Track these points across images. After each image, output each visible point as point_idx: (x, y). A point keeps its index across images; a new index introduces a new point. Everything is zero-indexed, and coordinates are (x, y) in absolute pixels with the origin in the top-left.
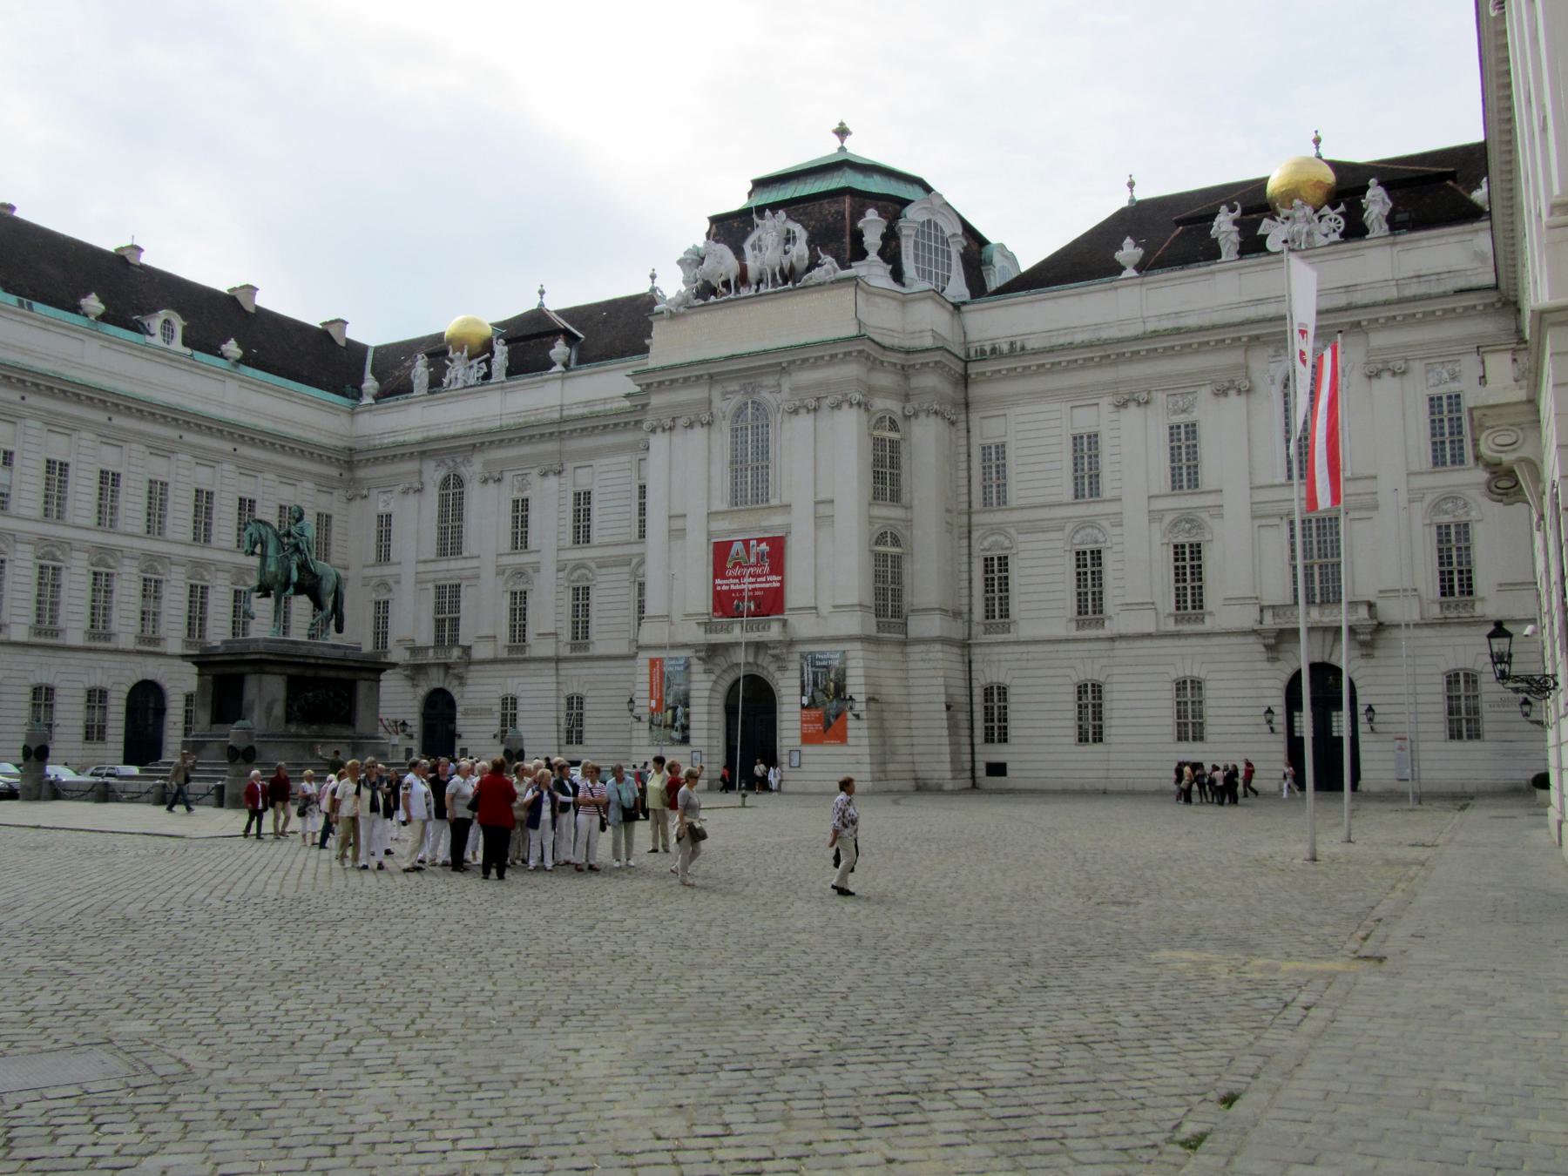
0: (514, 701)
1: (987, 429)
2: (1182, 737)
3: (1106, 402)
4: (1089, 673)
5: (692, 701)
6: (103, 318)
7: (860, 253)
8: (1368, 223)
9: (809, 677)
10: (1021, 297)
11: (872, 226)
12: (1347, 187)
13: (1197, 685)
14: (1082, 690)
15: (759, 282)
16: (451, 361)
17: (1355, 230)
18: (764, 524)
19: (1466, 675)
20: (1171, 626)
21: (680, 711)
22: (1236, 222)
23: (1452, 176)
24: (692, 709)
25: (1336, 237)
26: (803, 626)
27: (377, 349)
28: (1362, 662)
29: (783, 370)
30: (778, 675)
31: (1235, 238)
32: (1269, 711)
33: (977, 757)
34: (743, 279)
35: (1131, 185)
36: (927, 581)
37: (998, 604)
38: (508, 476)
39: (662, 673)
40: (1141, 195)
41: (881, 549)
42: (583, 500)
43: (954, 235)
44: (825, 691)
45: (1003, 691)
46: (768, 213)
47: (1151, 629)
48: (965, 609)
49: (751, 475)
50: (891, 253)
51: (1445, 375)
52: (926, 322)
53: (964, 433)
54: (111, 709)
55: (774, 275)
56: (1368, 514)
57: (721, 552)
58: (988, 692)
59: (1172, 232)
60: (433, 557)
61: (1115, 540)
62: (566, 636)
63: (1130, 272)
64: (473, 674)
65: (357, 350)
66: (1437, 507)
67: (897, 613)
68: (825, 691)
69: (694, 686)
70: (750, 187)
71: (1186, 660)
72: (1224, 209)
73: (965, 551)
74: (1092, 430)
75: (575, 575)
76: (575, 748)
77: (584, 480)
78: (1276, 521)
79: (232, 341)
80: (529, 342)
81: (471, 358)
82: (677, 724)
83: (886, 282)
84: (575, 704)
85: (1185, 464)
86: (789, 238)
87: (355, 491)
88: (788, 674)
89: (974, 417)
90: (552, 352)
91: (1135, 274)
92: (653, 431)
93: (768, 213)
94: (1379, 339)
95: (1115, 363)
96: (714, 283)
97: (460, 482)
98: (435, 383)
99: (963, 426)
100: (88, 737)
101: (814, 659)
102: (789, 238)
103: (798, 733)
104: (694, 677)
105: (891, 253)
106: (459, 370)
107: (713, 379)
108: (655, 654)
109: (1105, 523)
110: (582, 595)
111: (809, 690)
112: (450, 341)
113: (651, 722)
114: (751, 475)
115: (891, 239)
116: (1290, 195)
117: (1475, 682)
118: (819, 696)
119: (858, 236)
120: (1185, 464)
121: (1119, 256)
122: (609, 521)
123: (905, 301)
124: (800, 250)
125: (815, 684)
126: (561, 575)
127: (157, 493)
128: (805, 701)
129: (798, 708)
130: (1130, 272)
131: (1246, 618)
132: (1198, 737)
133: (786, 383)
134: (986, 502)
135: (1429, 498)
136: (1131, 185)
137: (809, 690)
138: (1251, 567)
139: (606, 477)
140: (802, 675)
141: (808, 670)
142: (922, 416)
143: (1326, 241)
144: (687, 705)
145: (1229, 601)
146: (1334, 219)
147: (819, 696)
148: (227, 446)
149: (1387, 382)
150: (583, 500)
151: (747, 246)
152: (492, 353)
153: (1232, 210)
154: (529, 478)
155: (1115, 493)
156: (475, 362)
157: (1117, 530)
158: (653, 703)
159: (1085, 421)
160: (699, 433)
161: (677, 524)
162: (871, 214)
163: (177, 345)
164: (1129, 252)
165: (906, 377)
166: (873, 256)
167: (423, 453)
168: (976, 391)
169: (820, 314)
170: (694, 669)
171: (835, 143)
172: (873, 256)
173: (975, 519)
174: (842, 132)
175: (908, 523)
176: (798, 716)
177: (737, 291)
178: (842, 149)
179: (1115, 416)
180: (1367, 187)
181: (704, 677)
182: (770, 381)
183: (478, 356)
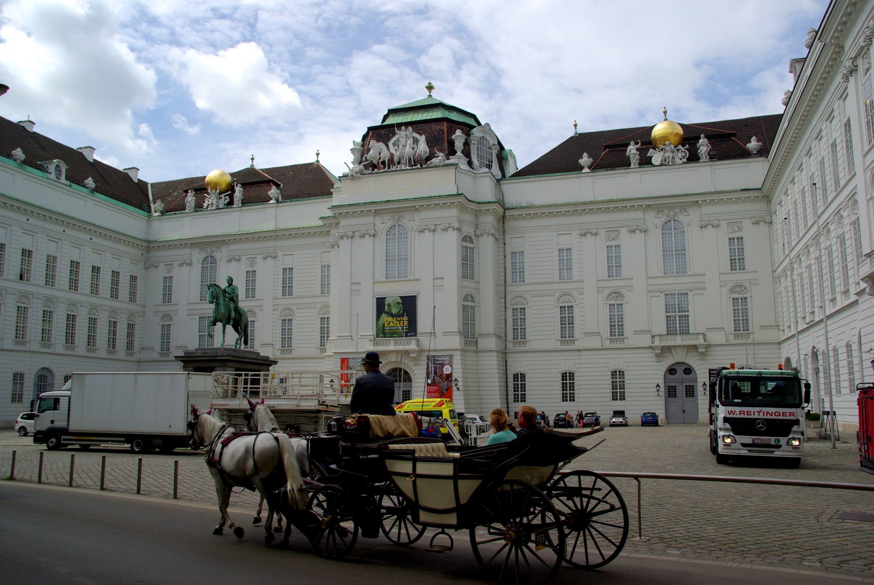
1: (514, 244)
2: (614, 398)
3: (575, 233)
4: (567, 367)
6: (25, 162)
7: (452, 152)
8: (700, 155)
10: (531, 178)
11: (458, 137)
12: (690, 136)
13: (622, 373)
14: (564, 376)
15: (399, 163)
16: (208, 194)
20: (607, 344)
22: (637, 149)
23: (734, 135)
25: (685, 160)
26: (426, 342)
27: (152, 185)
28: (700, 362)
29: (415, 209)
30: (414, 368)
31: (637, 157)
32: (658, 385)
33: (510, 409)
34: (391, 161)
35: (575, 126)
36: (487, 320)
37: (520, 333)
38: (244, 259)
40: (581, 130)
41: (466, 303)
42: (288, 272)
43: (494, 145)
45: (523, 376)
46: (403, 128)
47: (599, 346)
48: (503, 335)
49: (396, 263)
50: (467, 153)
51: (736, 229)
52: (483, 187)
53: (502, 245)
54: (26, 384)
55: (410, 160)
56: (701, 292)
57: (381, 303)
58: (516, 377)
59: (610, 150)
60: (199, 301)
63: (586, 170)
65: (142, 185)
66: (732, 290)
67: (473, 337)
68: (441, 376)
70: (386, 112)
71: (617, 361)
72: (632, 143)
73: (503, 305)
75: (283, 314)
77: (288, 262)
78: (659, 294)
79: (90, 179)
80: (253, 185)
81: (220, 193)
83: (464, 166)
85: (614, 266)
86: (416, 141)
87: (149, 265)
88: (419, 367)
89: (506, 237)
90: (269, 193)
91: (588, 170)
92: (342, 238)
93: (403, 128)
94: (707, 210)
95: (580, 214)
96: (375, 162)
97: (214, 261)
98: (199, 207)
99: (502, 241)
100: (13, 400)
102: (416, 141)
105: (467, 153)
106: (210, 200)
109: (575, 293)
110: (287, 324)
112: (208, 184)
114: (396, 263)
115: (466, 144)
116: (664, 138)
118: (437, 379)
119: (451, 143)
120: (614, 266)
121: (581, 161)
122: (306, 282)
123: (476, 176)
124: (423, 147)
125: (435, 373)
126: (275, 312)
127: (51, 261)
128: (430, 381)
130: (586, 170)
131: (646, 341)
132: (623, 398)
134: (514, 281)
135: (729, 285)
136: (575, 126)
138: (645, 316)
139: (305, 261)
140: (428, 368)
141: (432, 366)
142: (485, 236)
143: (681, 162)
145: (637, 332)
146: (682, 153)
147: (437, 379)
148: (88, 237)
150: (288, 272)
151: (390, 144)
152: (234, 191)
153: (636, 143)
156: (223, 195)
157: (582, 296)
159: (564, 241)
160: (368, 240)
161: (355, 287)
162: (458, 132)
163: (63, 179)
164: (585, 160)
165: (477, 216)
166: (459, 153)
167: (192, 244)
168: (509, 224)
169: (439, 181)
171: (427, 92)
172: (459, 153)
173: (508, 288)
174: (430, 88)
175: (478, 289)
177: (389, 167)
178: (430, 96)
180: (699, 138)
182: (408, 215)
183: (224, 192)
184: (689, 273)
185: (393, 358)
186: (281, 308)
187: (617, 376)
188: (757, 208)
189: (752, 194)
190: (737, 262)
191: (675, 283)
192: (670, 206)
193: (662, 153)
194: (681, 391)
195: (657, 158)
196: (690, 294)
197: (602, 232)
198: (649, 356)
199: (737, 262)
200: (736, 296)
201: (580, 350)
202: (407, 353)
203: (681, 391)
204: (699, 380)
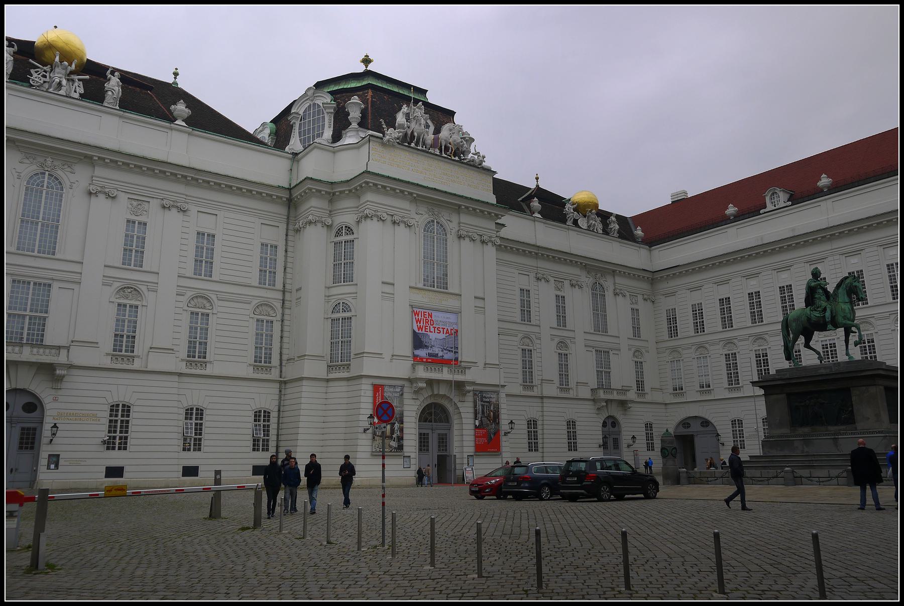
0: (127, 409)
3: (532, 275)
5: (405, 419)
9: (479, 408)
17: (606, 232)
21: (397, 426)
24: (405, 425)
29: (458, 209)
38: (123, 198)
39: (382, 396)
42: (205, 239)
44: (488, 417)
61: (538, 346)
62: (183, 353)
64: (77, 382)
68: (488, 417)
69: (406, 408)
74: (528, 288)
76: (192, 454)
78: (591, 349)
82: (394, 436)
84: (195, 414)
88: (465, 404)
101: (482, 397)
103: (473, 444)
104: (406, 402)
107: (416, 200)
108: (378, 382)
109: (534, 337)
110: (199, 319)
111: (479, 416)
113: (374, 434)
125: (483, 411)
126: (180, 298)
128: (477, 423)
129: (472, 427)
133: (455, 218)
135: (633, 349)
137: (479, 416)
140: (475, 406)
144: (402, 422)
149: (620, 298)
150: (205, 239)
154: (146, 205)
155: (538, 322)
156: (76, 77)
157: (538, 341)
160: (401, 230)
170: (405, 395)
176: (472, 432)
179: (536, 284)
181: (412, 402)
184: (609, 334)
185: (443, 391)
186: (190, 294)
187: (571, 424)
188: (644, 286)
189: (647, 275)
190: (636, 331)
191: (601, 340)
192: (597, 269)
193: (585, 220)
194: (610, 443)
195: (582, 222)
196: (611, 353)
197: (552, 280)
198: (589, 408)
200: (636, 359)
201: (542, 398)
202: (460, 386)
203: (610, 443)
204: (623, 433)
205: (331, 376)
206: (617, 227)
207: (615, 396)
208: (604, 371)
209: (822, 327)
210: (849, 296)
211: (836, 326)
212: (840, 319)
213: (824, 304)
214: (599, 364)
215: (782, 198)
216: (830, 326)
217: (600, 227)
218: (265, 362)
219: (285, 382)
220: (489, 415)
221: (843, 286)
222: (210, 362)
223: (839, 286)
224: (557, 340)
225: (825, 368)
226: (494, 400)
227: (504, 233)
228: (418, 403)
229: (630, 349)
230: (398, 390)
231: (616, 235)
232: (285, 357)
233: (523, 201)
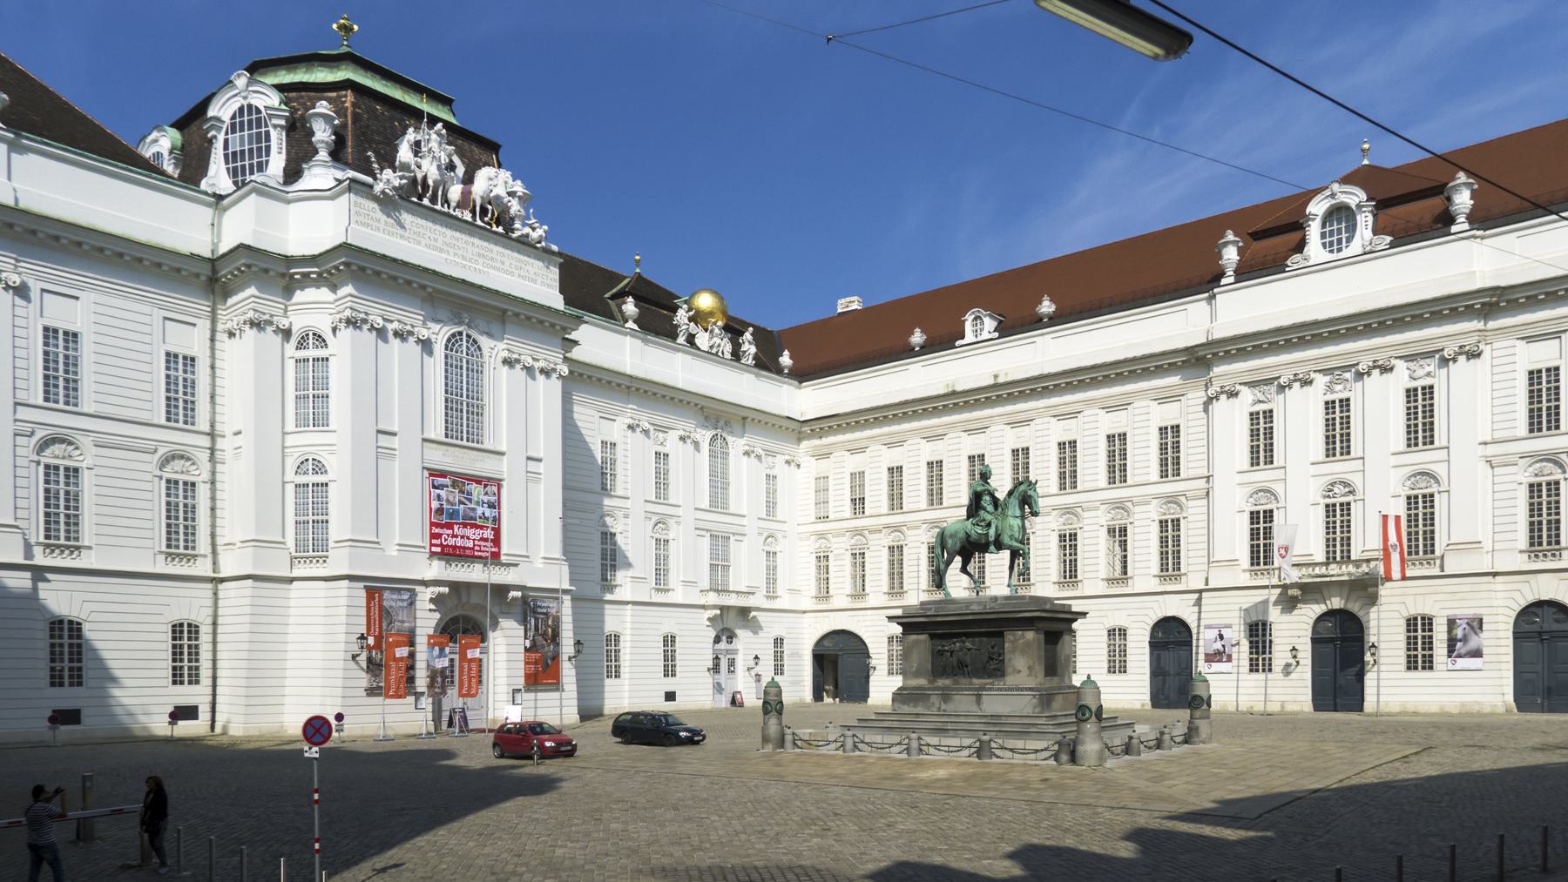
18: (478, 465)
19: (190, 625)
39: (381, 606)
63: (630, 324)
69: (419, 623)
104: (419, 614)
117: (197, 632)
158: (371, 641)
170: (419, 605)
191: (717, 520)
195: (703, 340)
199: (771, 505)
202: (501, 590)
205: (296, 573)
206: (753, 350)
207: (733, 601)
208: (719, 567)
209: (983, 547)
210: (1022, 509)
211: (999, 546)
212: (1006, 540)
213: (989, 517)
214: (714, 554)
215: (989, 324)
216: (992, 548)
217: (727, 347)
218: (186, 548)
219: (223, 580)
220: (545, 633)
221: (1016, 494)
222: (90, 548)
223: (1010, 493)
224: (655, 519)
225: (979, 603)
226: (553, 611)
227: (576, 353)
228: (437, 615)
229: (760, 534)
230: (406, 597)
231: (751, 362)
232: (219, 541)
233: (613, 297)
